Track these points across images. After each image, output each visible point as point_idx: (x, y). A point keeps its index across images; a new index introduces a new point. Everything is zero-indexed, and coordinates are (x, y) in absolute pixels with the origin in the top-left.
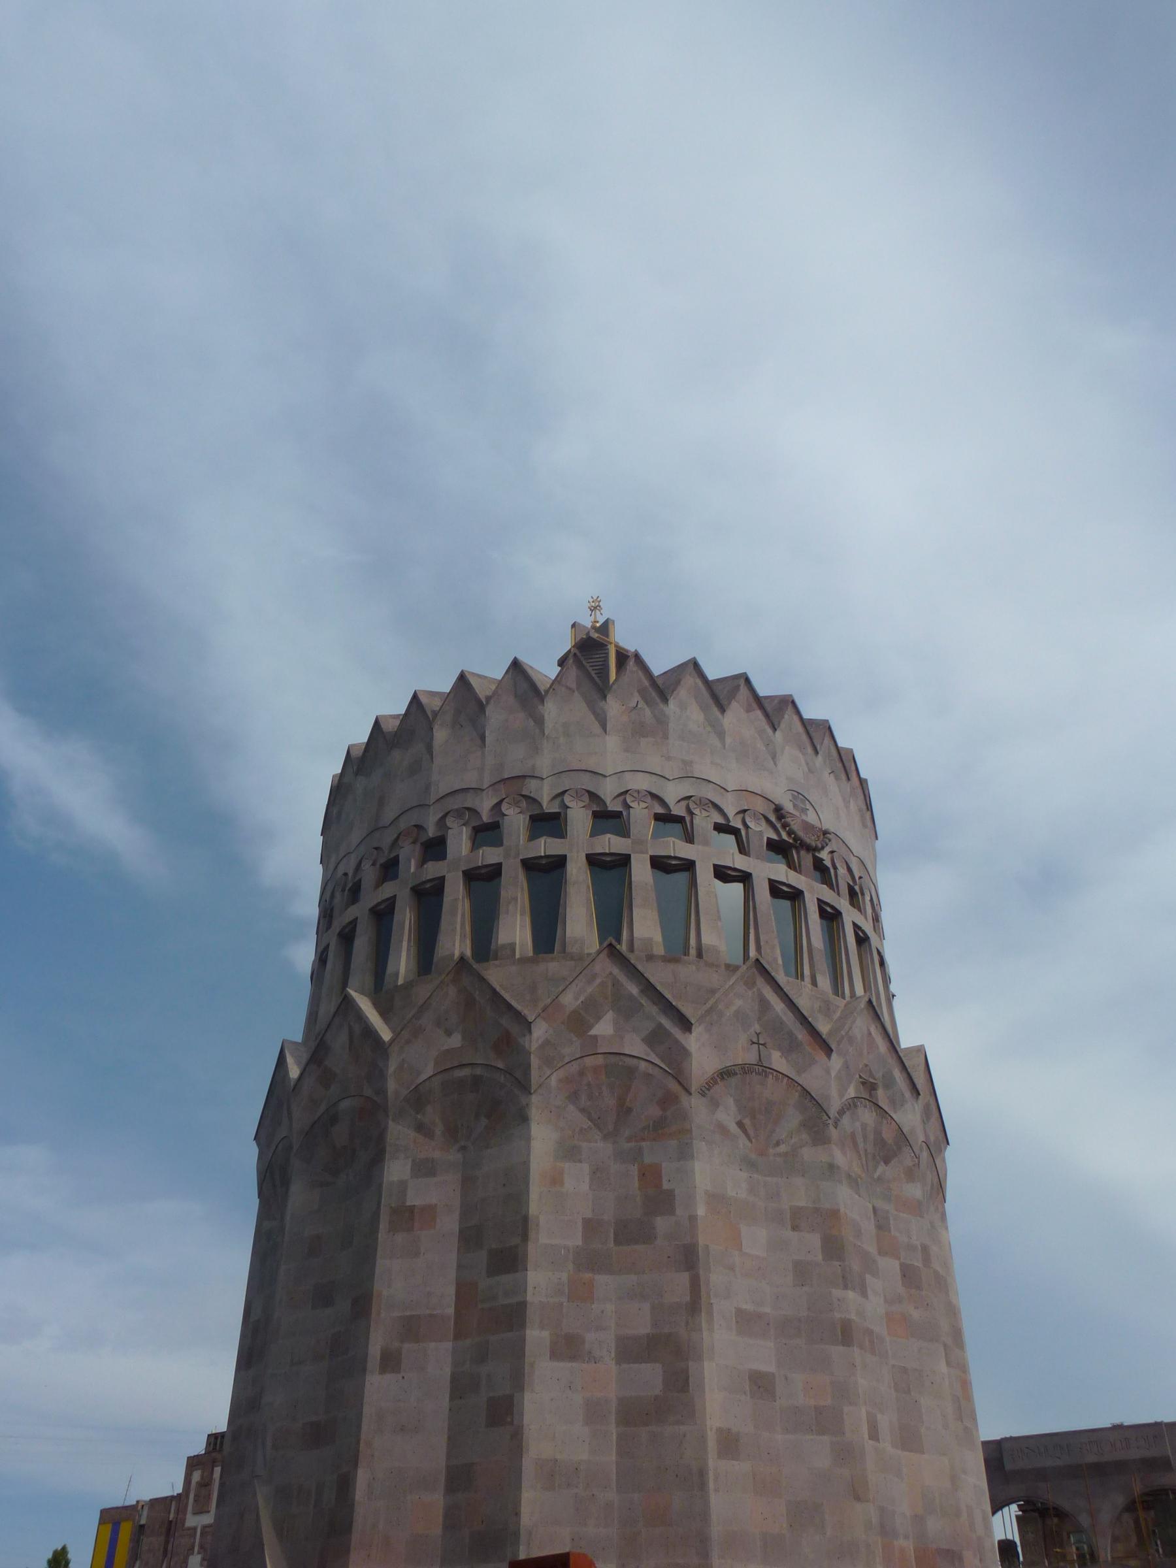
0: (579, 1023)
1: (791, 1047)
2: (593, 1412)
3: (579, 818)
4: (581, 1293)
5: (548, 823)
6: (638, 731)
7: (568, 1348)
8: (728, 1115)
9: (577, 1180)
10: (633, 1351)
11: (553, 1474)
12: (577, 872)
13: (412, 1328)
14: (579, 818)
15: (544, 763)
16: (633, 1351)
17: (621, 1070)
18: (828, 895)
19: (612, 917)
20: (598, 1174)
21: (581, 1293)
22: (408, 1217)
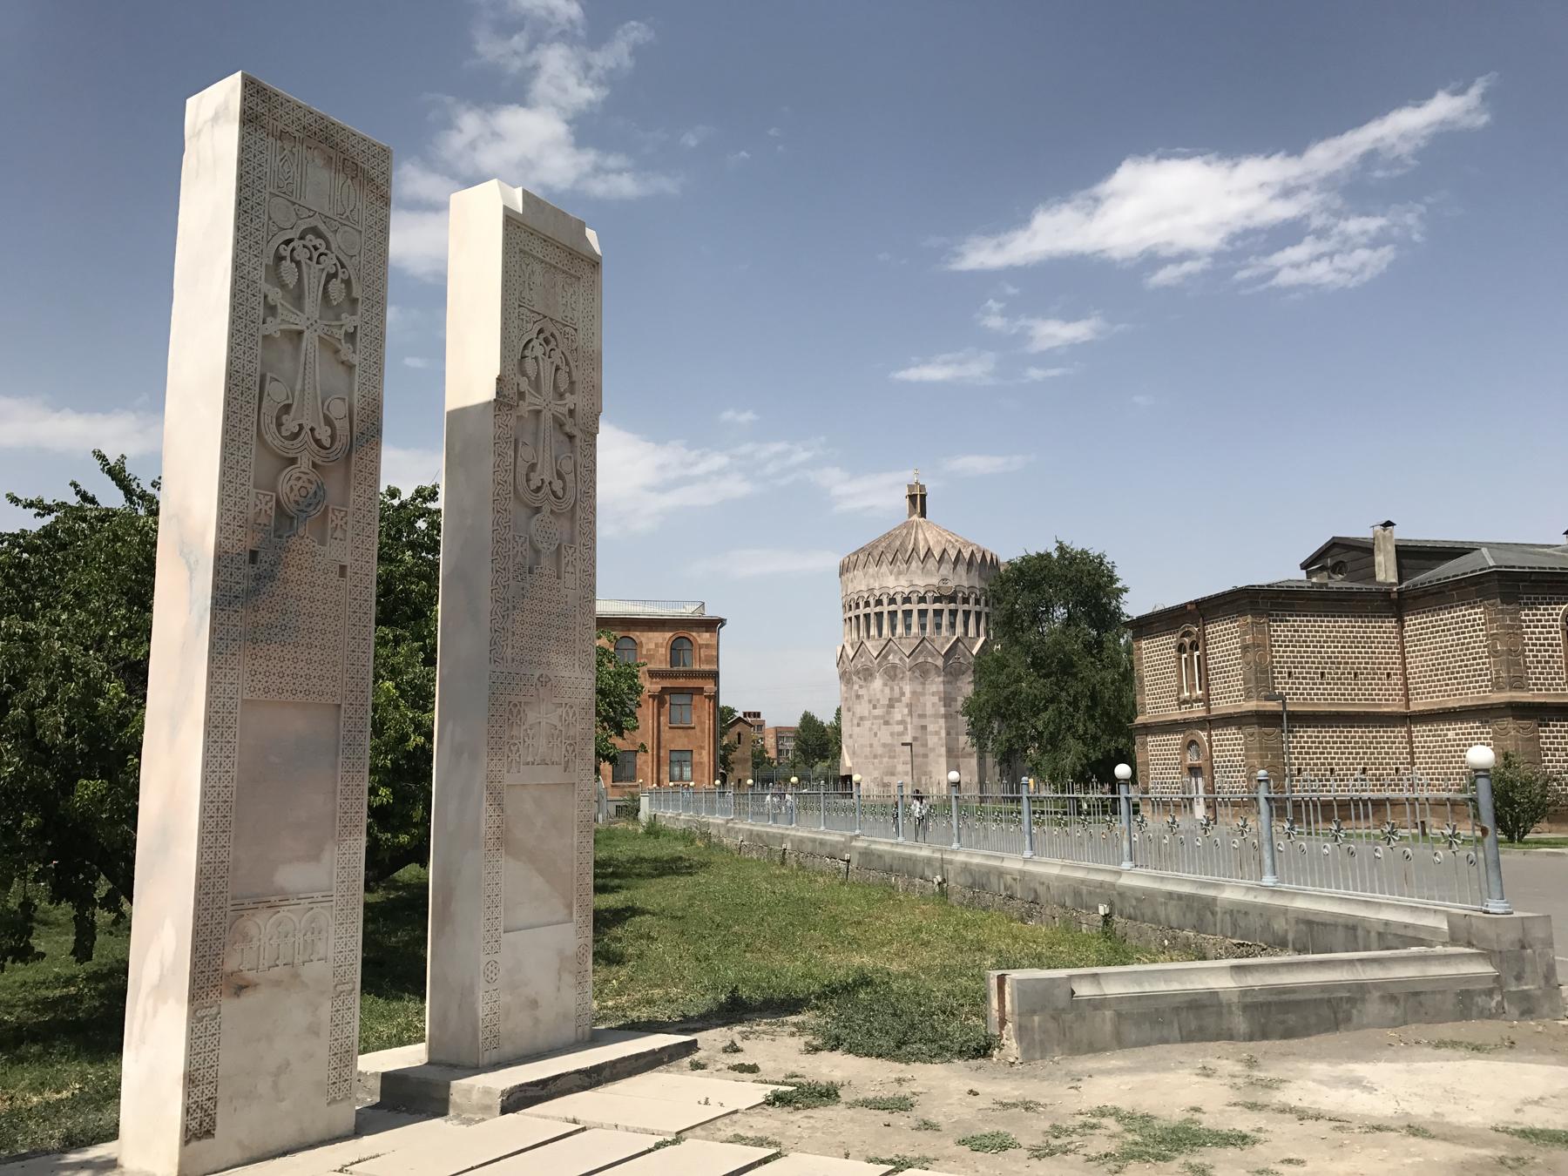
0: (885, 657)
1: (933, 656)
2: (892, 734)
3: (885, 601)
4: (888, 713)
5: (879, 602)
6: (900, 573)
7: (887, 723)
8: (917, 674)
9: (887, 690)
10: (899, 723)
11: (884, 745)
12: (885, 615)
13: (862, 718)
14: (885, 601)
15: (877, 586)
16: (899, 723)
17: (894, 667)
18: (952, 606)
19: (893, 628)
20: (892, 689)
21: (888, 713)
22: (858, 697)
